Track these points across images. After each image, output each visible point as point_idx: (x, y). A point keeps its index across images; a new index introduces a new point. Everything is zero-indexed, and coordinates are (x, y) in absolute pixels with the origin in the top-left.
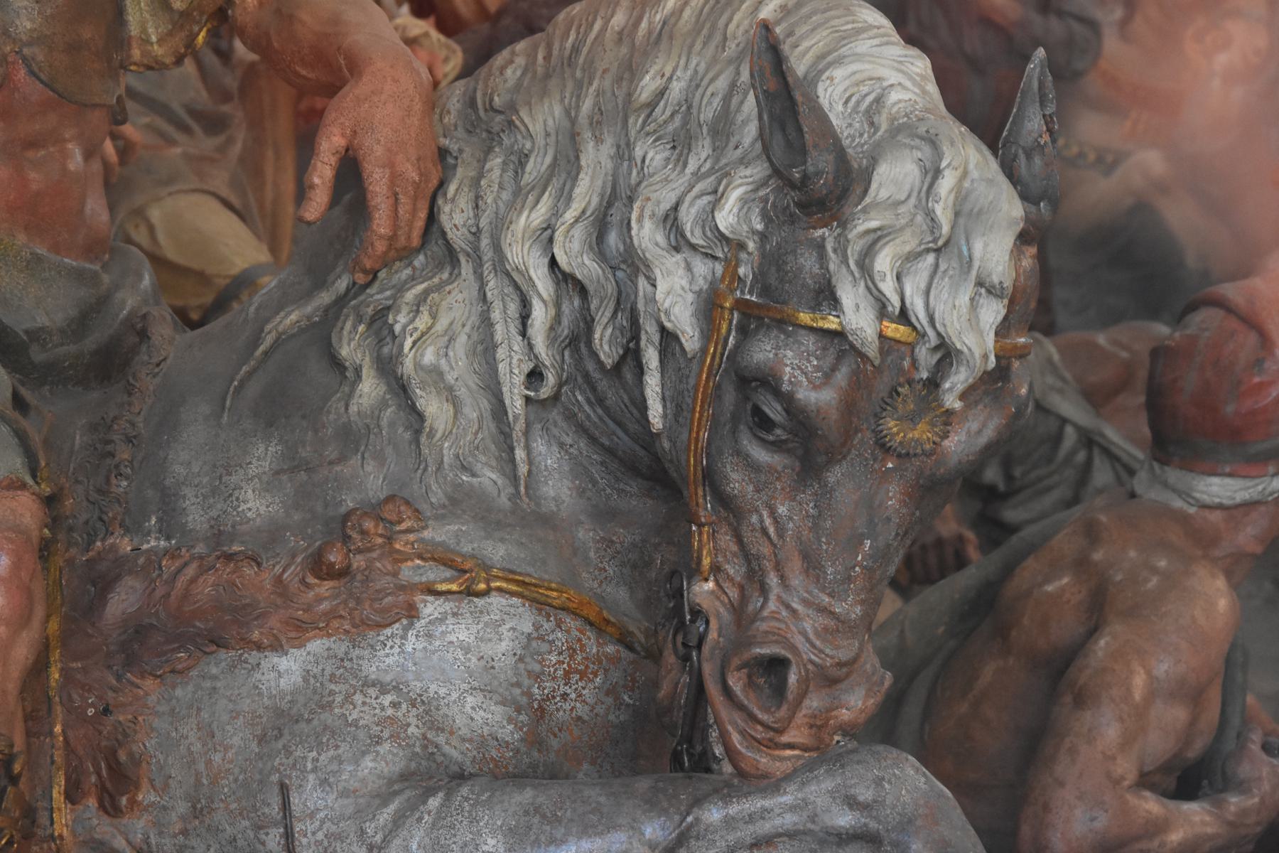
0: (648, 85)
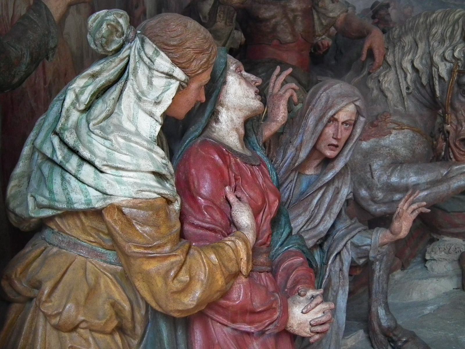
0: (434, 31)
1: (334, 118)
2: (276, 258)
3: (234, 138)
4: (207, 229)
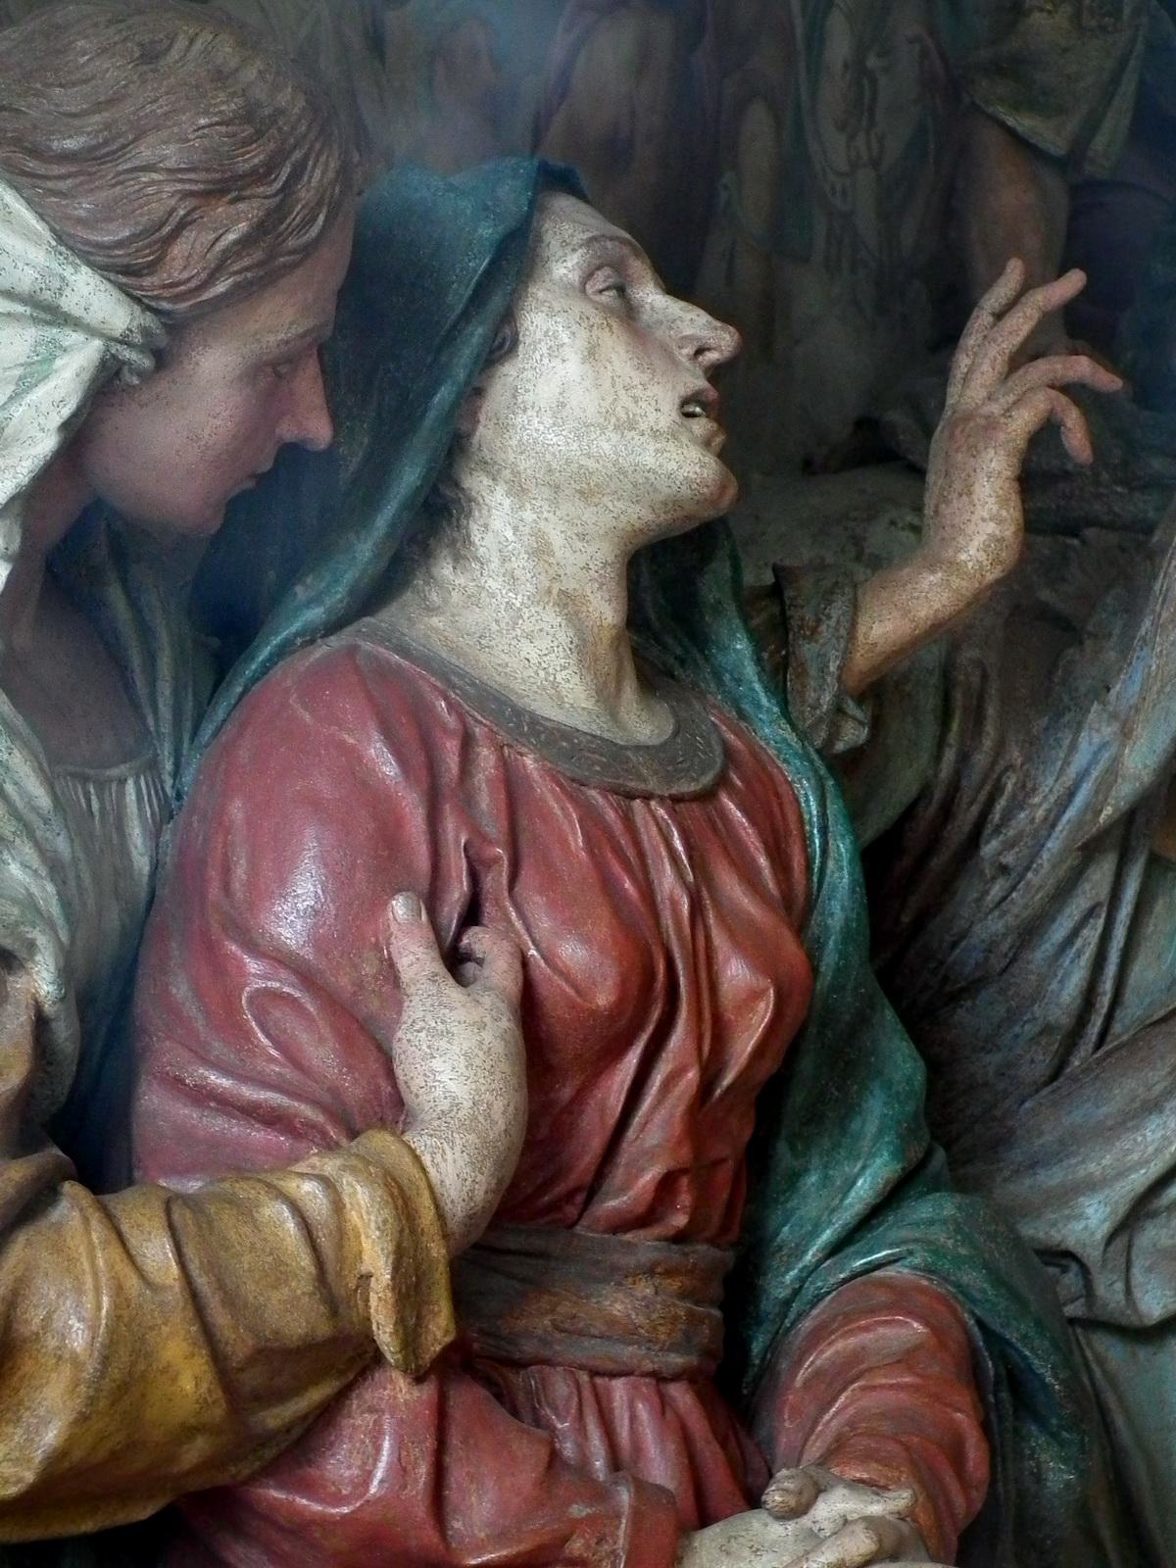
2: (800, 1316)
3: (544, 644)
4: (252, 1112)
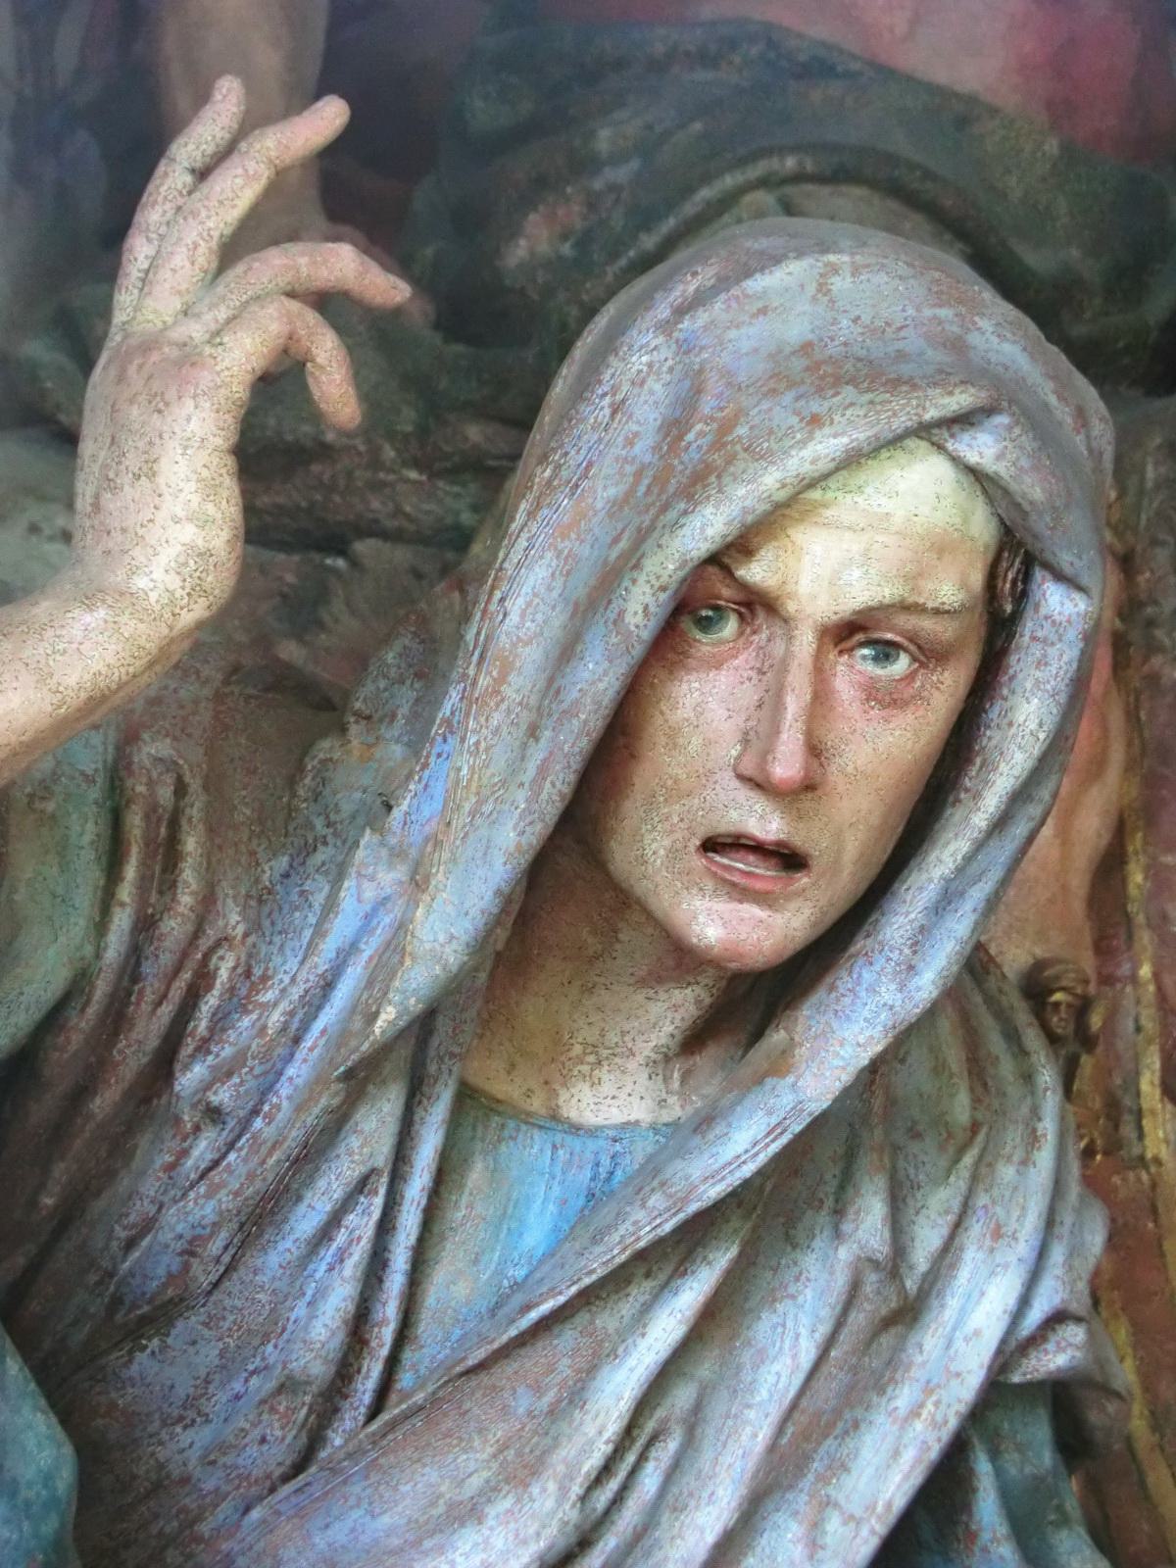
1: (743, 586)
